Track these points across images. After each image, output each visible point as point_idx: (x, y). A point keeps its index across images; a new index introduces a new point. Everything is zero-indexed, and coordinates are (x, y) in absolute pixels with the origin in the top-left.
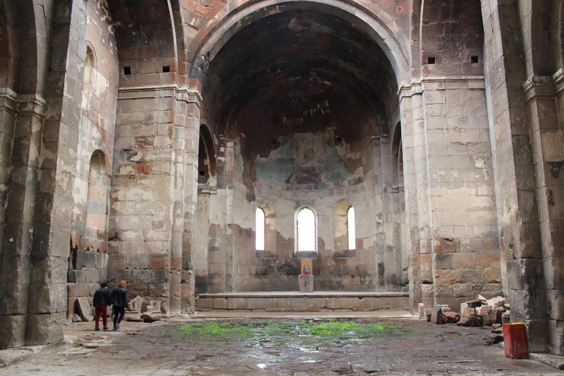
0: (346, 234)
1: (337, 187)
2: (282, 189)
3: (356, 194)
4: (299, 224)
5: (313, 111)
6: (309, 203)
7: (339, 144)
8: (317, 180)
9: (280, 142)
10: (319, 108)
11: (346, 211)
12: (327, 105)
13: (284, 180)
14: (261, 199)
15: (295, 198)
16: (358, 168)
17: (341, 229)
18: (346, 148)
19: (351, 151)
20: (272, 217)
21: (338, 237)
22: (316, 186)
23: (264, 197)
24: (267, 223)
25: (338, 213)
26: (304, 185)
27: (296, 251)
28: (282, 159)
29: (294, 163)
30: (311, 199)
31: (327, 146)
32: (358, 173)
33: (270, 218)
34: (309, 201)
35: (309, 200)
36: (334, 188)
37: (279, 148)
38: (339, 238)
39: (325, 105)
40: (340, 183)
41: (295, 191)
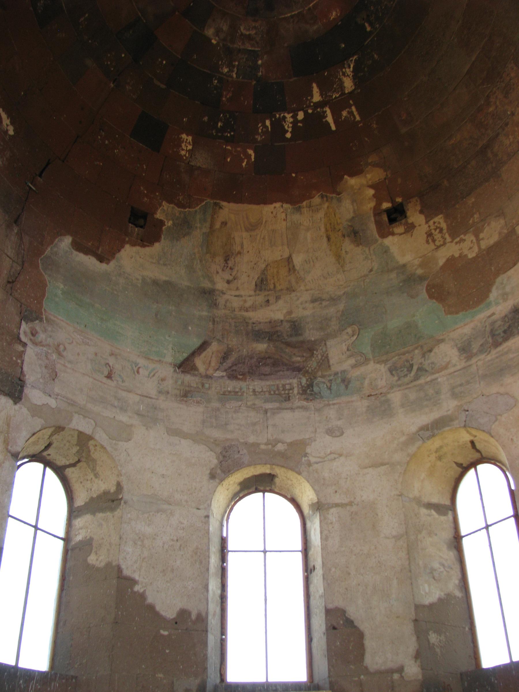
0: (459, 594)
1: (406, 380)
2: (160, 392)
3: (508, 380)
4: (231, 557)
5: (295, 117)
6: (282, 455)
7: (399, 229)
8: (313, 364)
9: (161, 223)
10: (318, 105)
11: (449, 489)
12: (348, 84)
13: (169, 359)
14: (53, 403)
15: (217, 434)
16: (499, 280)
17: (436, 565)
18: (429, 235)
19: (453, 239)
20: (102, 510)
21: (427, 601)
22: (310, 386)
23: (73, 403)
24: (79, 538)
25: (416, 493)
26: (257, 384)
27: (213, 678)
28: (168, 283)
29: (214, 305)
30: (289, 438)
31: (348, 245)
32: (505, 296)
33: (94, 513)
34: (280, 447)
35: (278, 441)
36: (392, 387)
37: (157, 245)
38: (431, 606)
39: (341, 86)
40: (417, 359)
41: (216, 404)
